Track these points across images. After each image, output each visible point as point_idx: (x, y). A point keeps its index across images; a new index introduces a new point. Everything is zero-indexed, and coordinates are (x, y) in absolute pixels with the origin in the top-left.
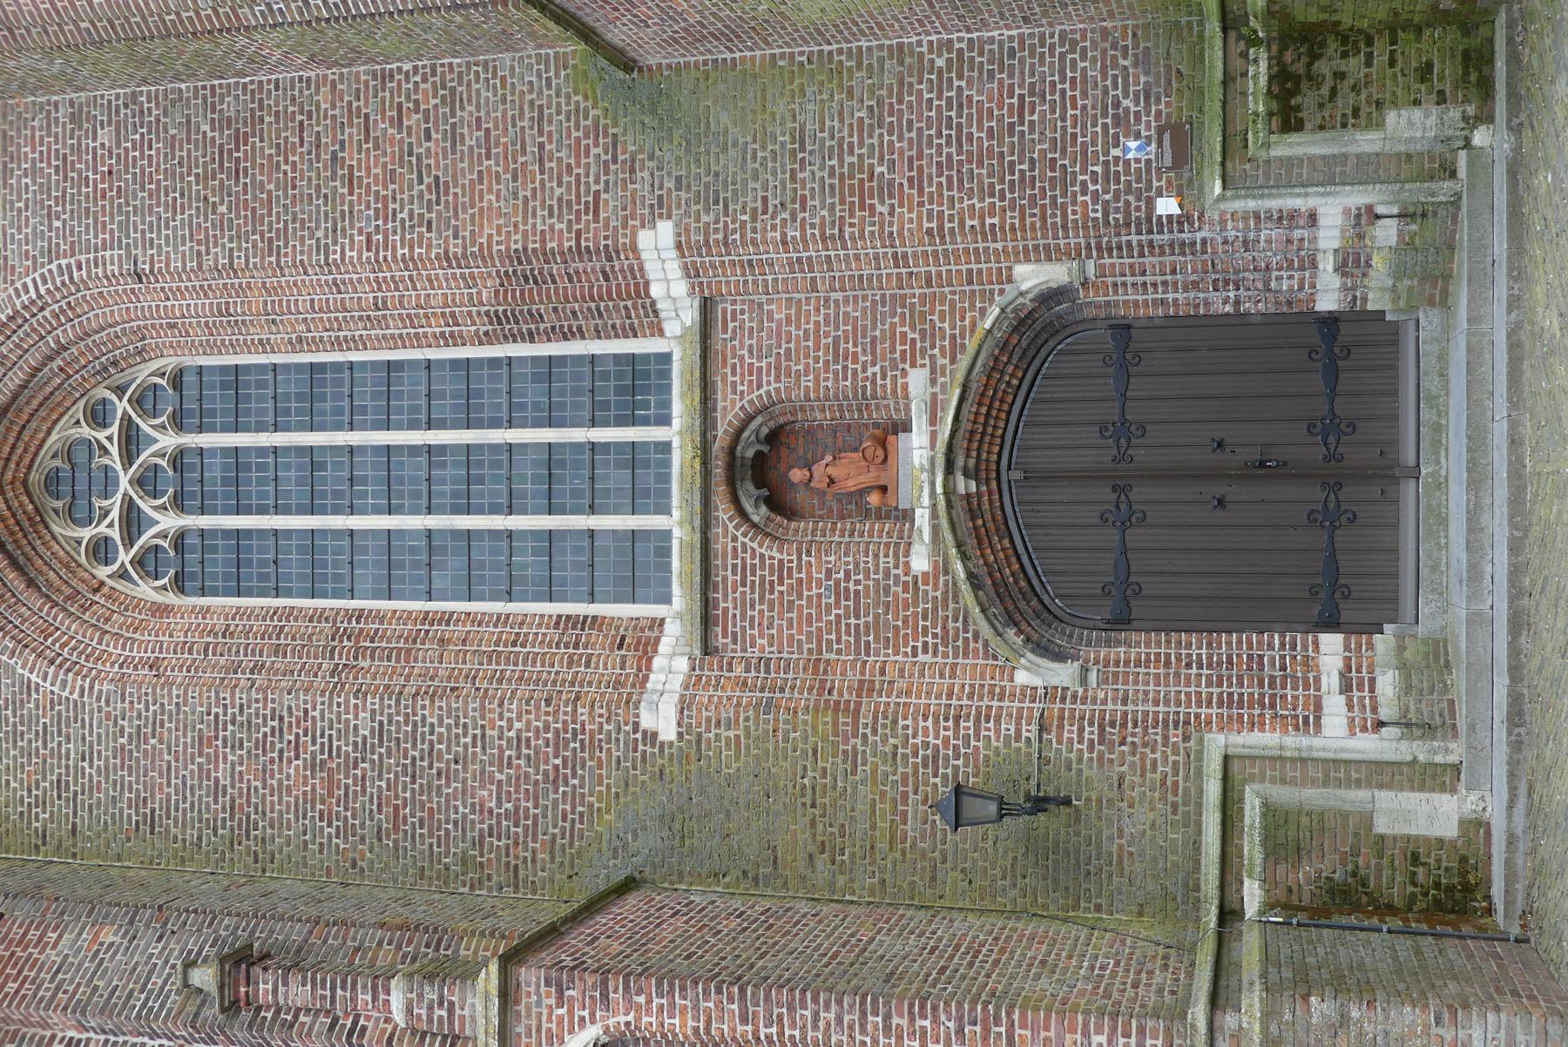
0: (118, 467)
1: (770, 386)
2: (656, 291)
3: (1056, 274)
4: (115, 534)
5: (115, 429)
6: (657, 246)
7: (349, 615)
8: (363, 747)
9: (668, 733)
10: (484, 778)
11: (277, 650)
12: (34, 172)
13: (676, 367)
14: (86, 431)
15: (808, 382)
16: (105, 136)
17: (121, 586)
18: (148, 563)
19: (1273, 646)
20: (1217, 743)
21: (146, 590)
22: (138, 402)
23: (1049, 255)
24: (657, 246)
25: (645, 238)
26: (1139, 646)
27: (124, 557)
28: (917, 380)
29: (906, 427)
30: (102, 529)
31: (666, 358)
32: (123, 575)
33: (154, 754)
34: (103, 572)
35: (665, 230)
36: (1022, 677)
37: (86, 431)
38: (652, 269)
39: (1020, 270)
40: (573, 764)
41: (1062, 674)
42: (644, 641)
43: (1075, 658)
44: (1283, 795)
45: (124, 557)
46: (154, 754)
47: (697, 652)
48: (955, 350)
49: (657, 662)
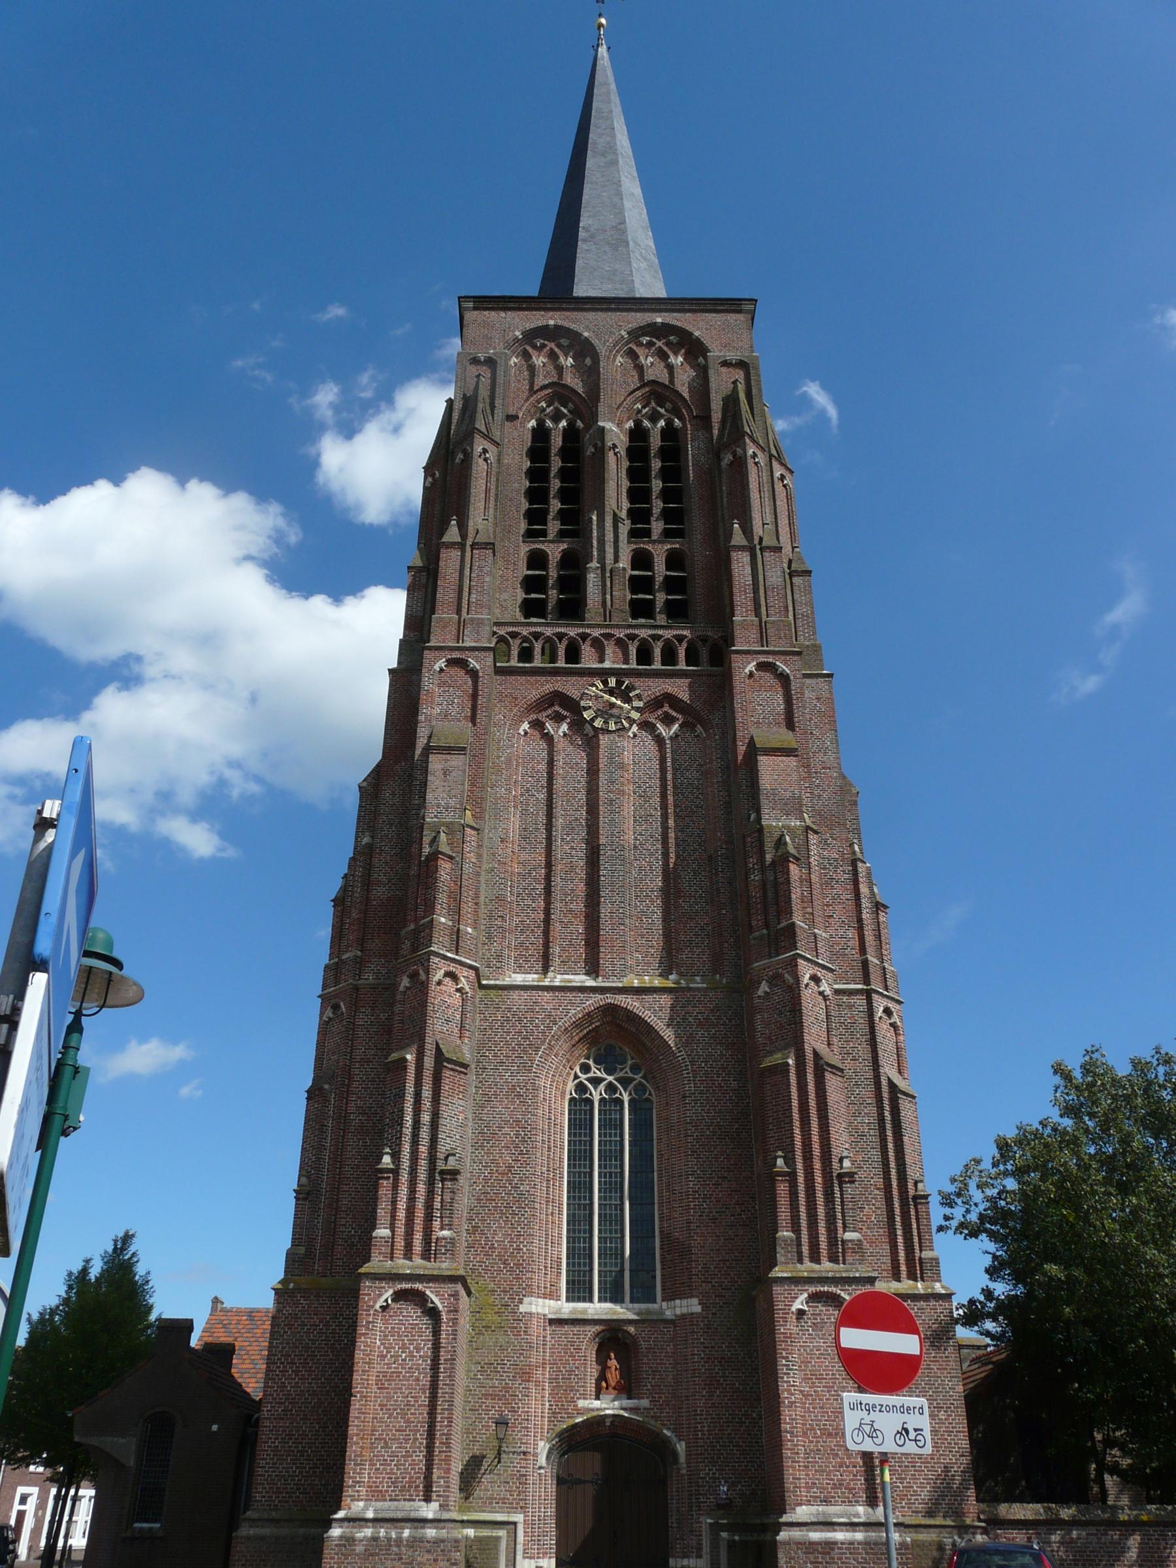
0: (617, 1076)
1: (643, 1345)
2: (678, 1302)
3: (682, 1459)
4: (591, 1075)
5: (631, 1075)
6: (692, 1306)
7: (561, 1173)
8: (516, 1187)
9: (523, 1308)
10: (506, 1235)
11: (549, 1148)
12: (722, 1055)
13: (650, 1306)
14: (630, 1062)
15: (645, 1360)
16: (734, 1084)
17: (572, 1077)
18: (581, 1088)
19: (551, 1541)
20: (519, 1518)
21: (571, 1085)
22: (640, 1083)
23: (689, 1454)
24: (692, 1306)
25: (695, 1301)
26: (551, 1487)
27: (583, 1077)
28: (645, 1403)
29: (629, 1398)
30: (593, 1069)
31: (655, 1302)
32: (576, 1077)
33: (513, 1103)
34: (577, 1069)
35: (698, 1309)
36: (541, 1444)
37: (630, 1062)
38: (685, 1302)
39: (683, 1443)
40: (511, 1271)
41: (542, 1460)
42: (552, 1295)
43: (548, 1464)
44: (503, 1545)
45: (583, 1077)
46: (513, 1103)
47: (550, 1316)
48: (655, 1418)
49: (547, 1301)
